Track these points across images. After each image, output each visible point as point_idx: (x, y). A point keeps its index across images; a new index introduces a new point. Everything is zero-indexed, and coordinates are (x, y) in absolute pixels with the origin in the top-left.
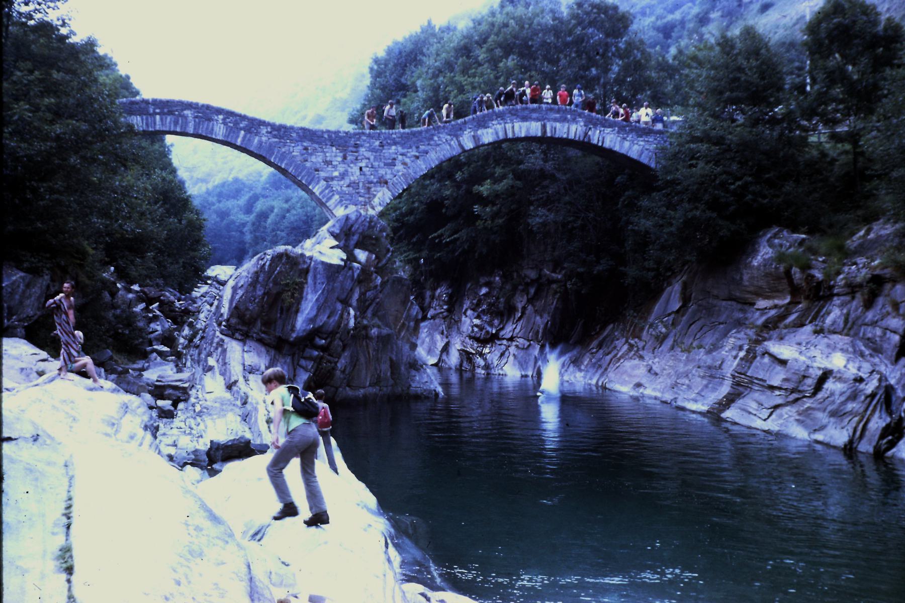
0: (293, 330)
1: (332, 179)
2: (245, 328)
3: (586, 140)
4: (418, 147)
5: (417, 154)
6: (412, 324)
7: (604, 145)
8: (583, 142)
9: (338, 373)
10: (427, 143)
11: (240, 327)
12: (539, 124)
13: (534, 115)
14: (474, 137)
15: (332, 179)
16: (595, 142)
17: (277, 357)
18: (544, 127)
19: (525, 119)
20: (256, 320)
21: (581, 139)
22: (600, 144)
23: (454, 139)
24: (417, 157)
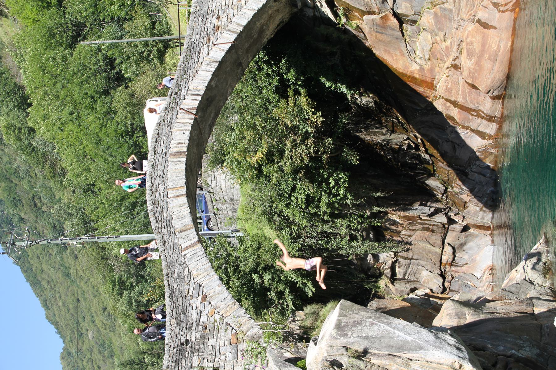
3: (194, 112)
4: (192, 297)
5: (200, 297)
7: (202, 93)
8: (196, 114)
10: (186, 287)
12: (172, 159)
13: (160, 167)
14: (181, 232)
16: (197, 103)
18: (174, 154)
19: (164, 176)
21: (193, 116)
22: (200, 98)
23: (183, 254)
24: (205, 298)
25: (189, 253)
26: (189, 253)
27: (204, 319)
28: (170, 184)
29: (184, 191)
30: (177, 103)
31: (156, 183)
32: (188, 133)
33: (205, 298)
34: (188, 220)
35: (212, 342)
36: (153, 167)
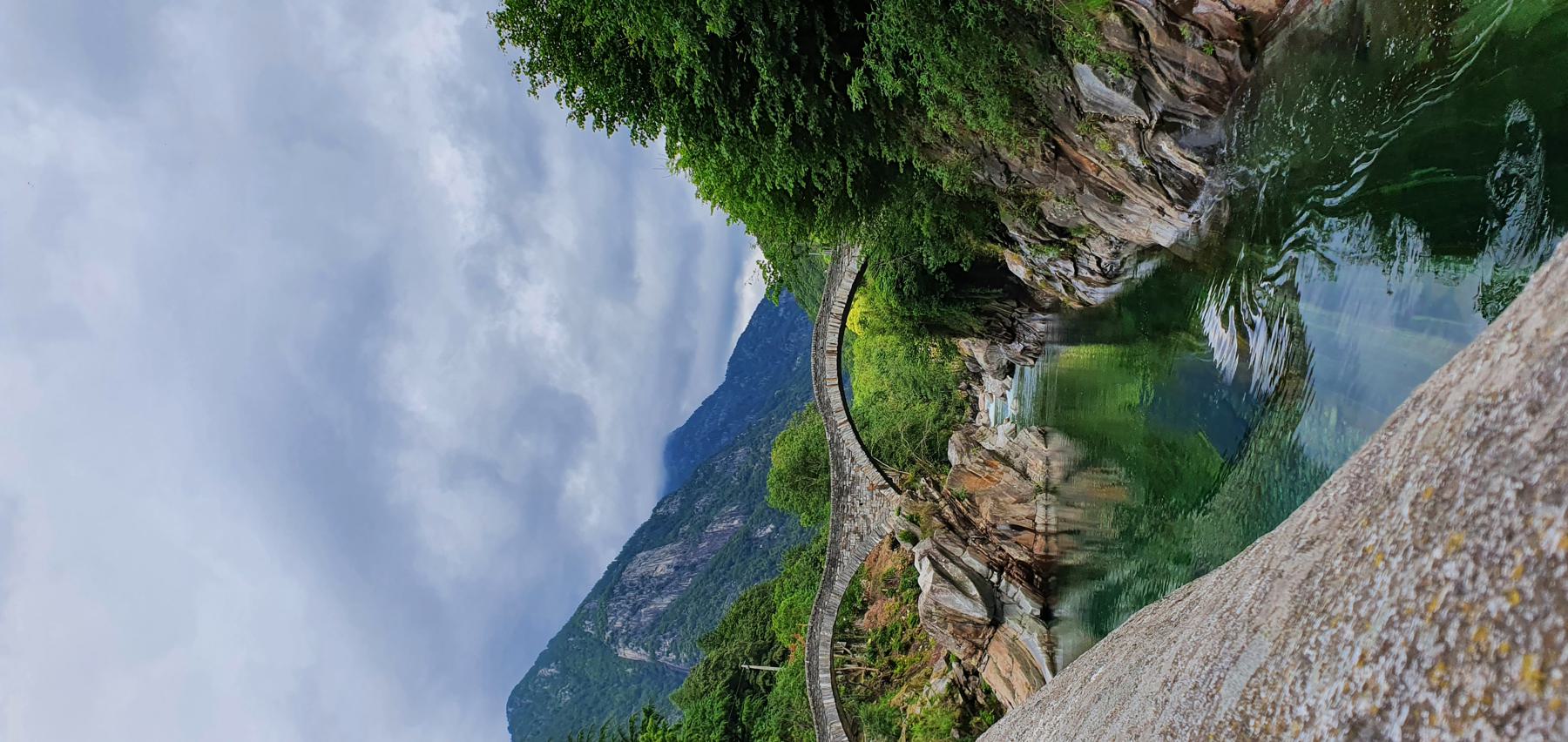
0: (983, 619)
1: (868, 528)
2: (980, 652)
6: (987, 468)
7: (845, 301)
9: (1022, 559)
11: (978, 657)
13: (821, 361)
15: (868, 528)
17: (1002, 629)
19: (823, 370)
20: (973, 643)
24: (853, 459)
25: (842, 427)
26: (842, 427)
27: (853, 472)
28: (828, 376)
29: (837, 382)
30: (829, 309)
31: (819, 372)
32: (837, 336)
33: (853, 459)
34: (840, 404)
35: (858, 488)
36: (816, 361)
